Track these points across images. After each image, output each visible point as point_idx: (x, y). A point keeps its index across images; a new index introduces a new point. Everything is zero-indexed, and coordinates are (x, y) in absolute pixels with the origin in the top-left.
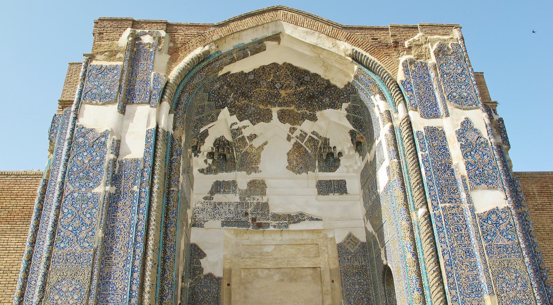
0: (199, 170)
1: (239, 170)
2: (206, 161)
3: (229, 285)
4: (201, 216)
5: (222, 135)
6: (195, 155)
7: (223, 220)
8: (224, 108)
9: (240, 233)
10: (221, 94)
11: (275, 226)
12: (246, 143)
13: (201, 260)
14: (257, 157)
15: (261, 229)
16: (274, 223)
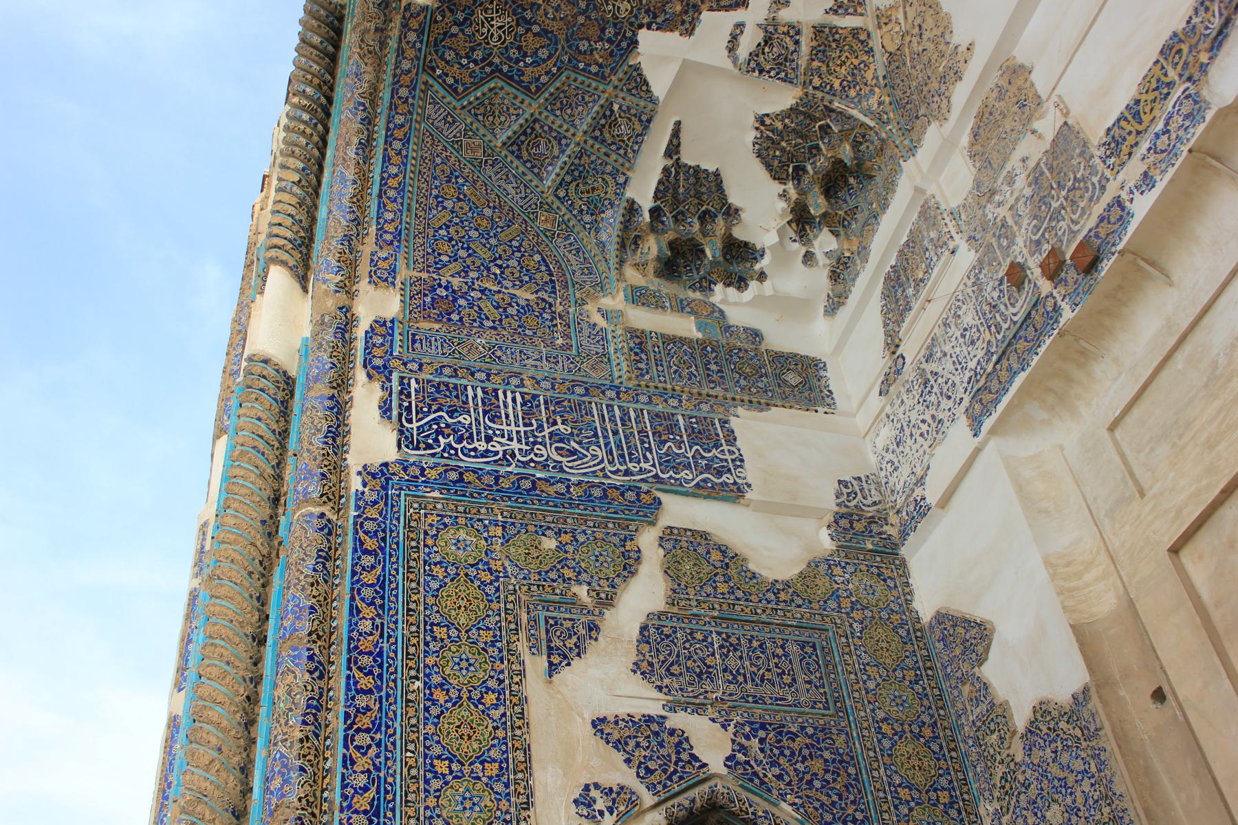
0: (827, 313)
1: (912, 151)
2: (809, 258)
3: (1159, 695)
4: (905, 470)
5: (751, 120)
6: (740, 283)
7: (966, 403)
8: (634, 43)
9: (1069, 380)
10: (554, 26)
11: (1147, 180)
12: (855, 32)
13: (988, 671)
14: (930, 23)
15: (1106, 266)
16: (1134, 169)
